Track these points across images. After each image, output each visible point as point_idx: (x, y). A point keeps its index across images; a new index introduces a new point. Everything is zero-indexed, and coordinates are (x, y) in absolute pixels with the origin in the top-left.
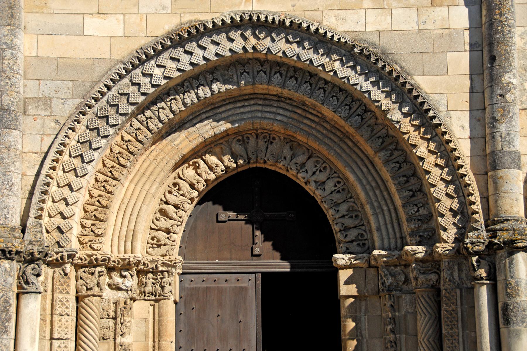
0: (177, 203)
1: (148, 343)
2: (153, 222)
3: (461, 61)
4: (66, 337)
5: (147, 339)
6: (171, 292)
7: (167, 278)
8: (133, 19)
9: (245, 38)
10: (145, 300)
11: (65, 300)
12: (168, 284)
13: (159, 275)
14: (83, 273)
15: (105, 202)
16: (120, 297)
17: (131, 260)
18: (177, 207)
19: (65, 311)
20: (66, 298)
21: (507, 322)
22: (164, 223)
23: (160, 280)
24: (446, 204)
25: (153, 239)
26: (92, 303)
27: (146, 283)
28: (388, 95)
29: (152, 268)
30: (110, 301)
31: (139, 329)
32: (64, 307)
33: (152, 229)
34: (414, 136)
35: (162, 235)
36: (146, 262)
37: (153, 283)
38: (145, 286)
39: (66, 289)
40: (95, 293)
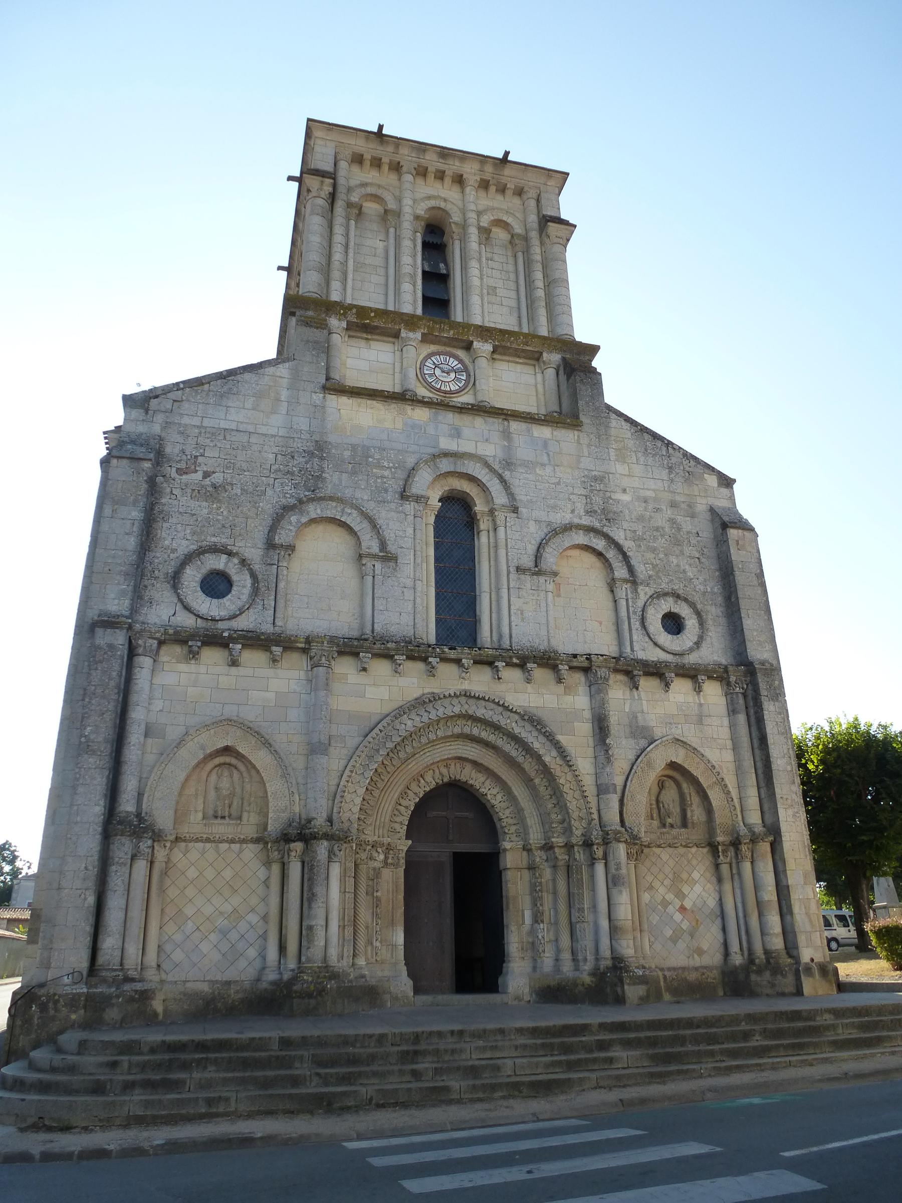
18: (406, 807)
22: (399, 819)
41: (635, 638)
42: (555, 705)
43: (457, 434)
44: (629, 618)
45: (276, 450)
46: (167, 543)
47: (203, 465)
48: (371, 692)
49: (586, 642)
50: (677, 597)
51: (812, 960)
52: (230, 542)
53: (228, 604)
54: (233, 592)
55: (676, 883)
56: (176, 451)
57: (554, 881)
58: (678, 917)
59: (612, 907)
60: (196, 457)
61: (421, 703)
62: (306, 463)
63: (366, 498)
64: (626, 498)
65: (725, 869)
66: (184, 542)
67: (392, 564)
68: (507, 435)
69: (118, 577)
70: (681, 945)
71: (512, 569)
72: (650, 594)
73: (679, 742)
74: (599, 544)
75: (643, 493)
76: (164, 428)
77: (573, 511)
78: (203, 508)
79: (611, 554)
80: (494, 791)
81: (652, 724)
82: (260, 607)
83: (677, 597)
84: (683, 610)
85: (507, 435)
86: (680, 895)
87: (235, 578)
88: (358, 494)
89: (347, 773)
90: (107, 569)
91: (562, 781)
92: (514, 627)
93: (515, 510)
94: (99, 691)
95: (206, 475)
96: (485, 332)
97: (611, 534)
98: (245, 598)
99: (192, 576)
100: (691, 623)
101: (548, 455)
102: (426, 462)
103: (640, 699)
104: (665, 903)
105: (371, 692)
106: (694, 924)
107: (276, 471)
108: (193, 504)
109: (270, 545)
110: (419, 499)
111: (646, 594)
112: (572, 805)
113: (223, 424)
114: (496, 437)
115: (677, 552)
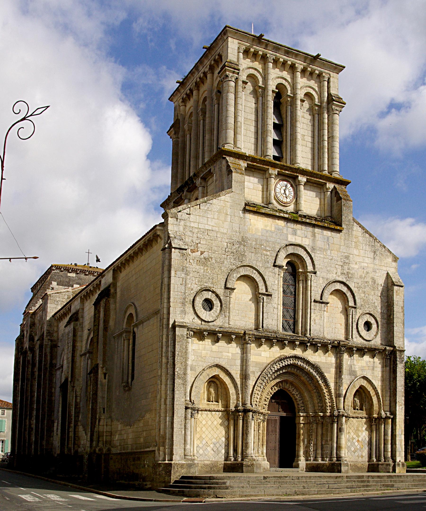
3: (333, 370)
8: (271, 353)
9: (290, 360)
21: (340, 431)
24: (328, 404)
28: (319, 377)
34: (324, 388)
41: (354, 333)
42: (325, 361)
43: (295, 233)
44: (352, 324)
45: (227, 241)
46: (189, 286)
47: (200, 248)
48: (263, 354)
49: (335, 333)
50: (371, 314)
51: (400, 461)
52: (212, 286)
53: (212, 314)
54: (214, 309)
55: (357, 430)
56: (190, 241)
57: (317, 428)
58: (356, 444)
59: (338, 439)
60: (197, 244)
61: (281, 359)
62: (239, 247)
63: (261, 265)
64: (356, 267)
65: (374, 427)
66: (196, 286)
67: (270, 297)
68: (314, 235)
69: (180, 305)
70: (356, 454)
71: (313, 300)
72: (361, 313)
73: (364, 378)
74: (345, 289)
75: (363, 265)
76: (184, 229)
77: (336, 273)
78: (201, 269)
79: (349, 294)
80: (297, 393)
81: (357, 370)
82: (224, 316)
83: (371, 314)
84: (373, 321)
85: (314, 235)
86: (358, 436)
87: (214, 302)
88: (258, 264)
89: (256, 386)
90: (175, 301)
91: (325, 391)
92: (312, 326)
93: (315, 273)
94: (180, 354)
95: (202, 253)
96: (304, 172)
97: (349, 285)
98: (218, 311)
99: (199, 301)
100: (374, 326)
101: (329, 245)
102: (283, 248)
103: (354, 359)
104: (353, 438)
105: (263, 354)
106: (361, 446)
107: (227, 252)
108: (198, 267)
109: (226, 288)
110: (280, 267)
111: (359, 313)
112: (327, 401)
113: (207, 227)
114: (309, 234)
115: (373, 294)
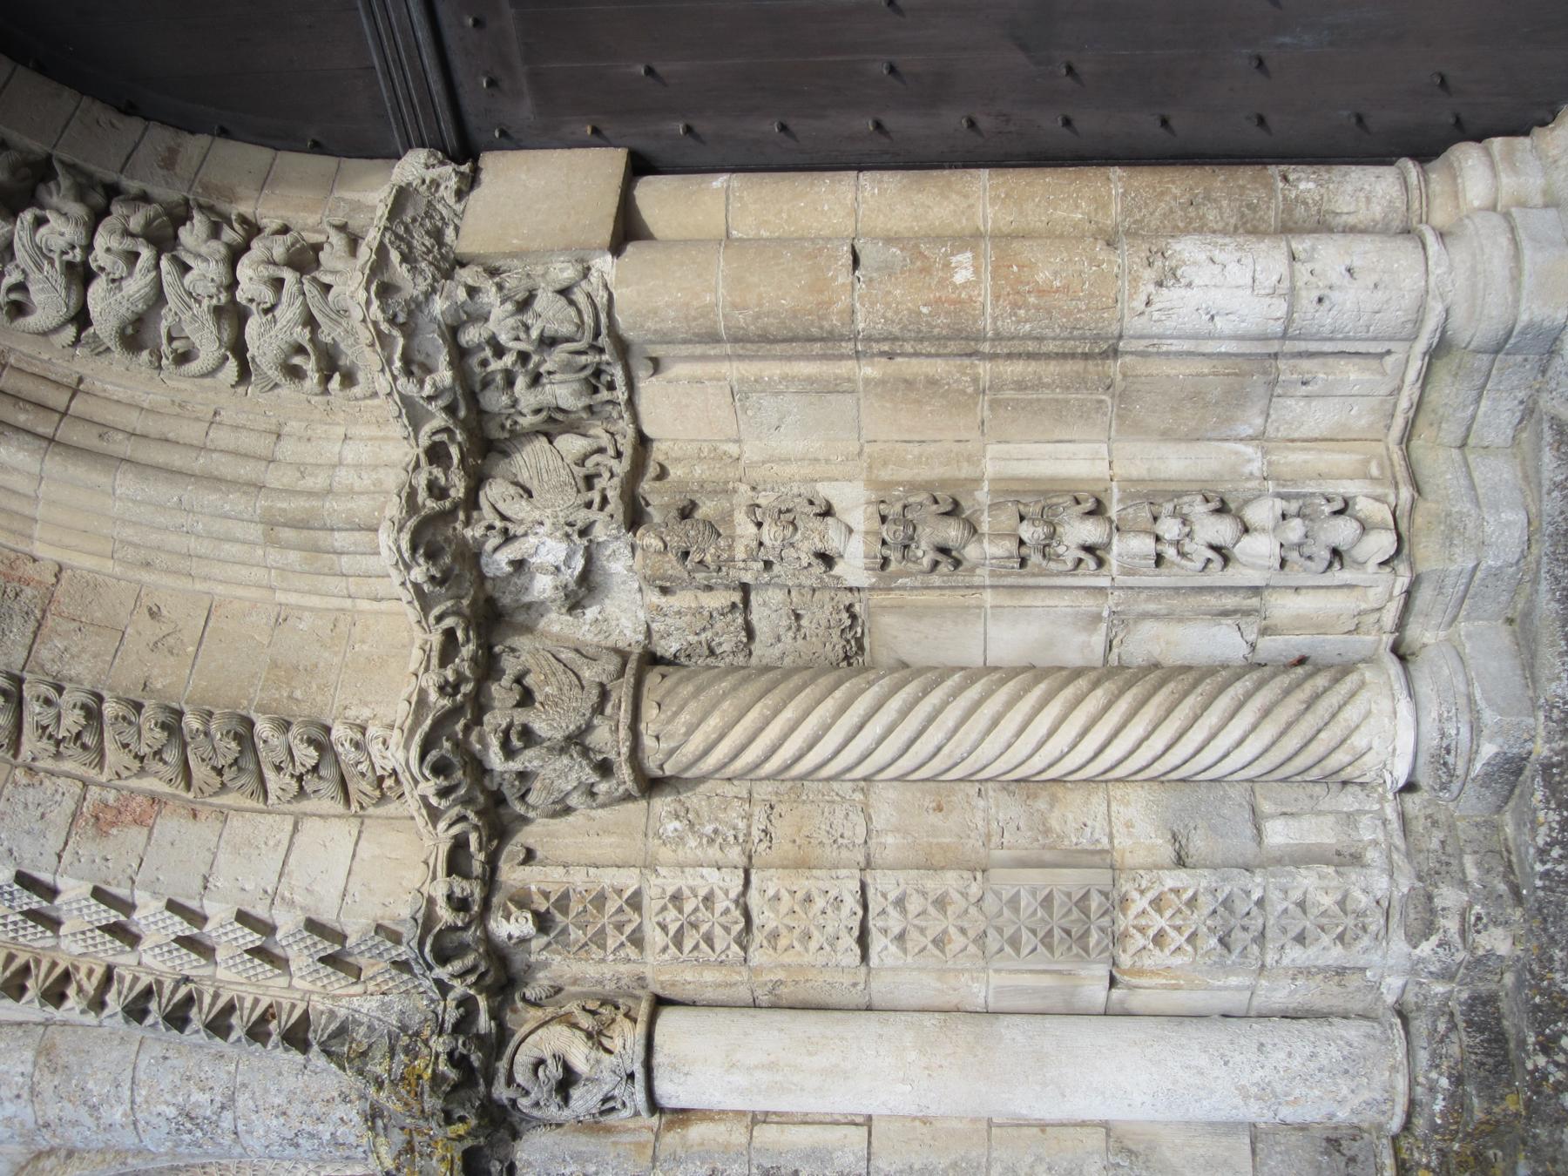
0: (61, 281)
1: (867, 381)
2: (212, 373)
4: (851, 903)
5: (846, 386)
6: (565, 292)
7: (492, 326)
10: (631, 403)
11: (672, 913)
12: (528, 318)
13: (484, 363)
14: (531, 799)
15: (146, 734)
16: (630, 569)
17: (418, 574)
19: (727, 911)
20: (664, 908)
23: (508, 360)
25: (295, 373)
26: (671, 753)
27: (537, 411)
29: (451, 410)
30: (659, 609)
31: (789, 420)
32: (703, 914)
33: (244, 373)
35: (265, 341)
36: (424, 441)
37: (536, 380)
38: (559, 409)
39: (620, 910)
40: (625, 750)
